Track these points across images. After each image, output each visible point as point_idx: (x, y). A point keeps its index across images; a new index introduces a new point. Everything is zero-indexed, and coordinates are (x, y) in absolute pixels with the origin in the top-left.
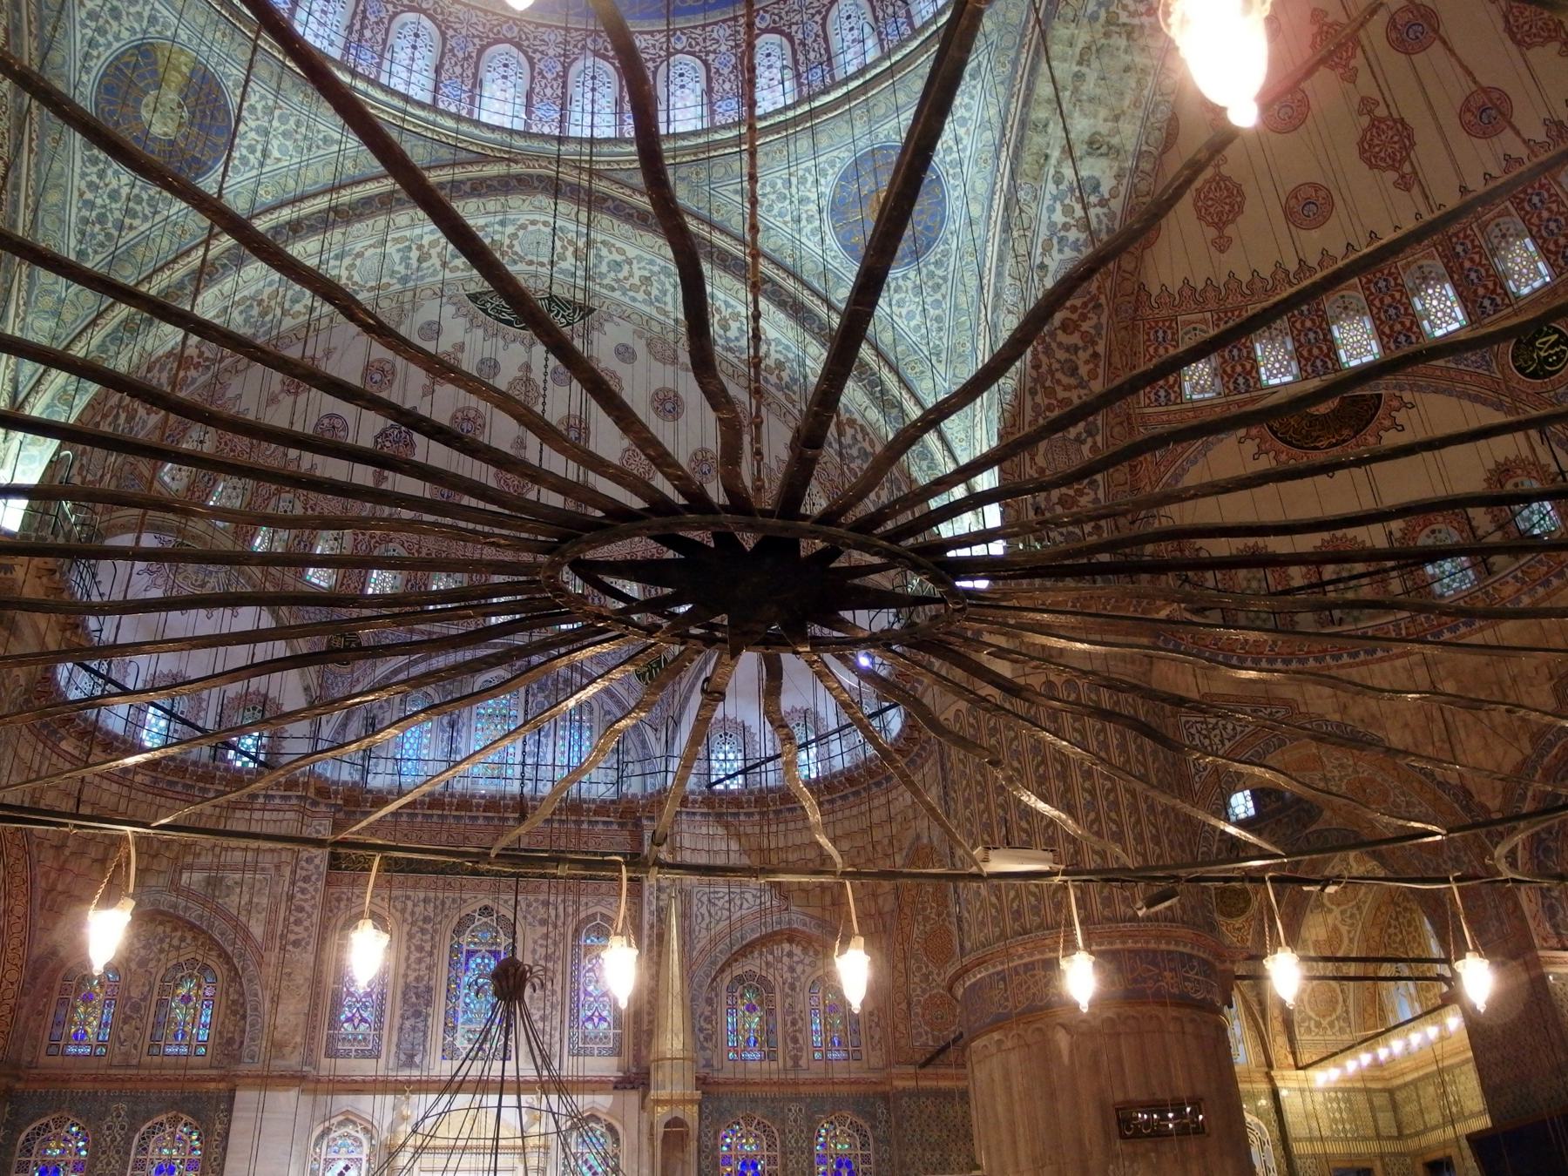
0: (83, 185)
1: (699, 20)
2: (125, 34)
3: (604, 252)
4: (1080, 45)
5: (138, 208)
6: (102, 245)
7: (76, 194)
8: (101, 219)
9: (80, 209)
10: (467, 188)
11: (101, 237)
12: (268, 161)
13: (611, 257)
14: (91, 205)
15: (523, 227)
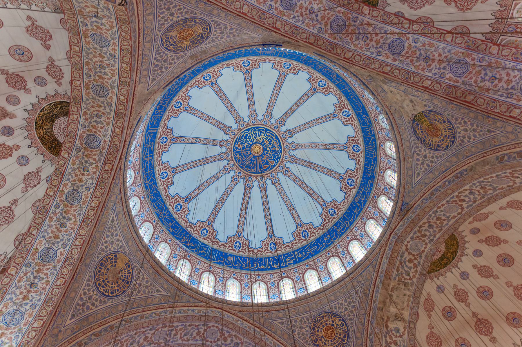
0: (83, 292)
1: (265, 272)
2: (112, 249)
3: (234, 339)
4: (391, 286)
5: (96, 303)
6: (80, 313)
7: (79, 295)
8: (84, 305)
9: (78, 300)
10: (196, 311)
11: (81, 311)
12: (139, 294)
13: (236, 341)
14: (81, 299)
15: (209, 327)
